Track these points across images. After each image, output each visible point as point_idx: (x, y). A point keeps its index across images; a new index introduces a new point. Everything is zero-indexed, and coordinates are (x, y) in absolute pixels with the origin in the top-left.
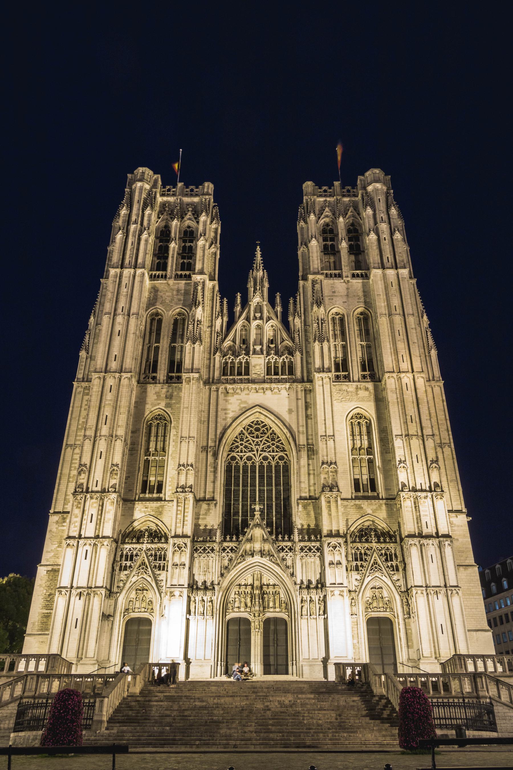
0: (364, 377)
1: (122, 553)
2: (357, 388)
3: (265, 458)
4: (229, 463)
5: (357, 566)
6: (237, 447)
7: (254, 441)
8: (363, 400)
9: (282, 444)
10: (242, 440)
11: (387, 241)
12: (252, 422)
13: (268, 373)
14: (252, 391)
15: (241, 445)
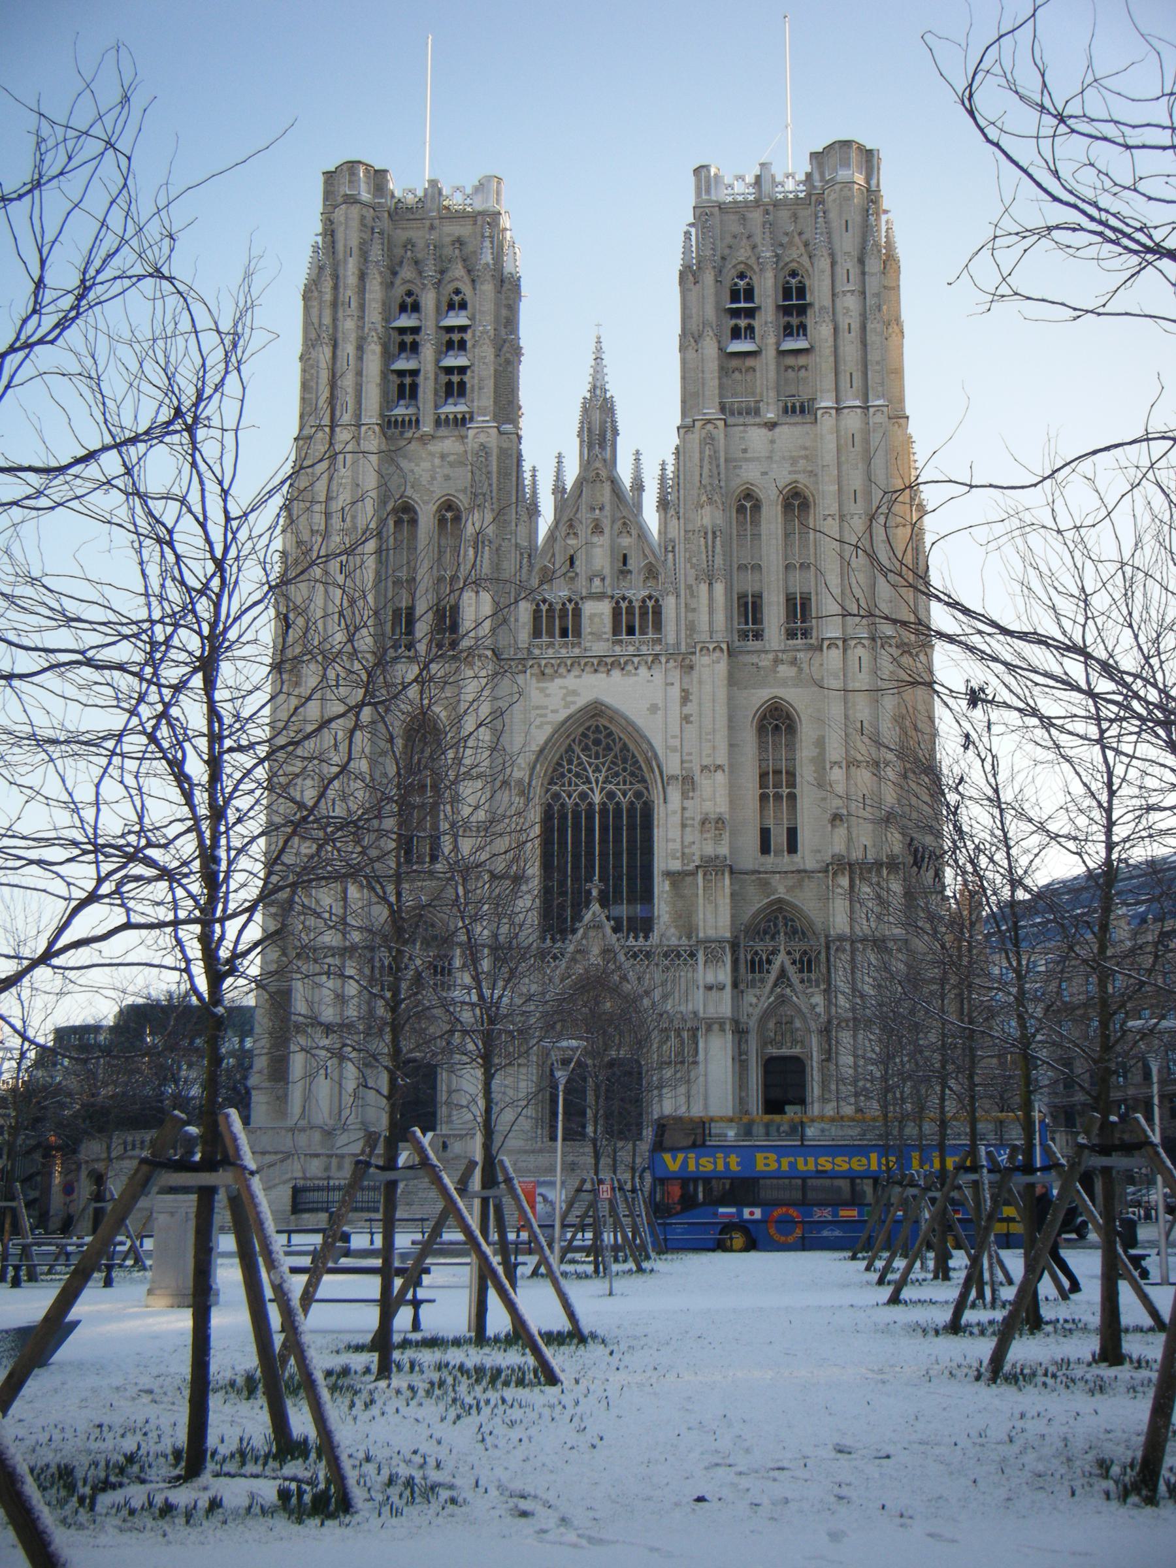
0: (791, 634)
1: (383, 966)
2: (777, 661)
3: (611, 795)
4: (549, 805)
5: (753, 980)
6: (563, 775)
7: (590, 764)
8: (784, 683)
9: (640, 768)
10: (570, 762)
11: (853, 334)
12: (588, 729)
13: (616, 631)
14: (588, 669)
15: (570, 771)
